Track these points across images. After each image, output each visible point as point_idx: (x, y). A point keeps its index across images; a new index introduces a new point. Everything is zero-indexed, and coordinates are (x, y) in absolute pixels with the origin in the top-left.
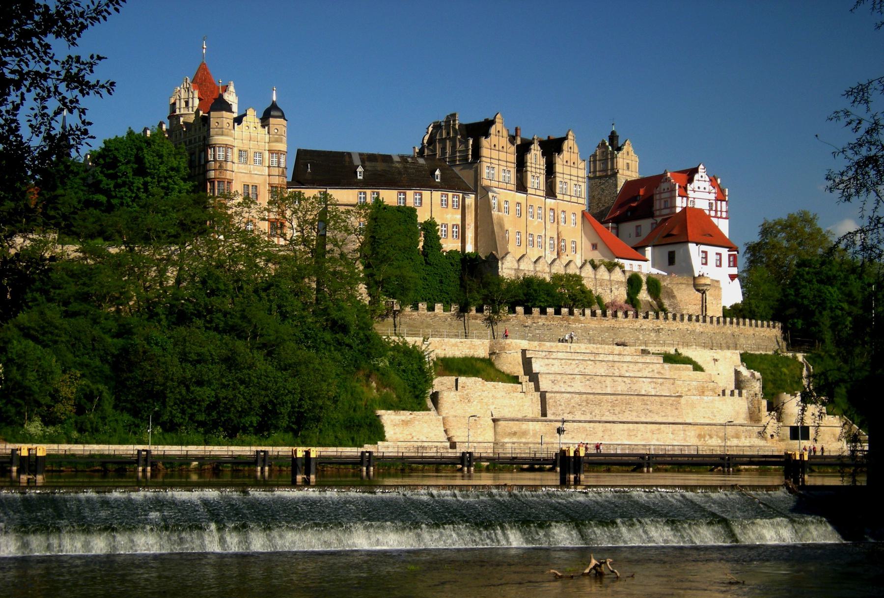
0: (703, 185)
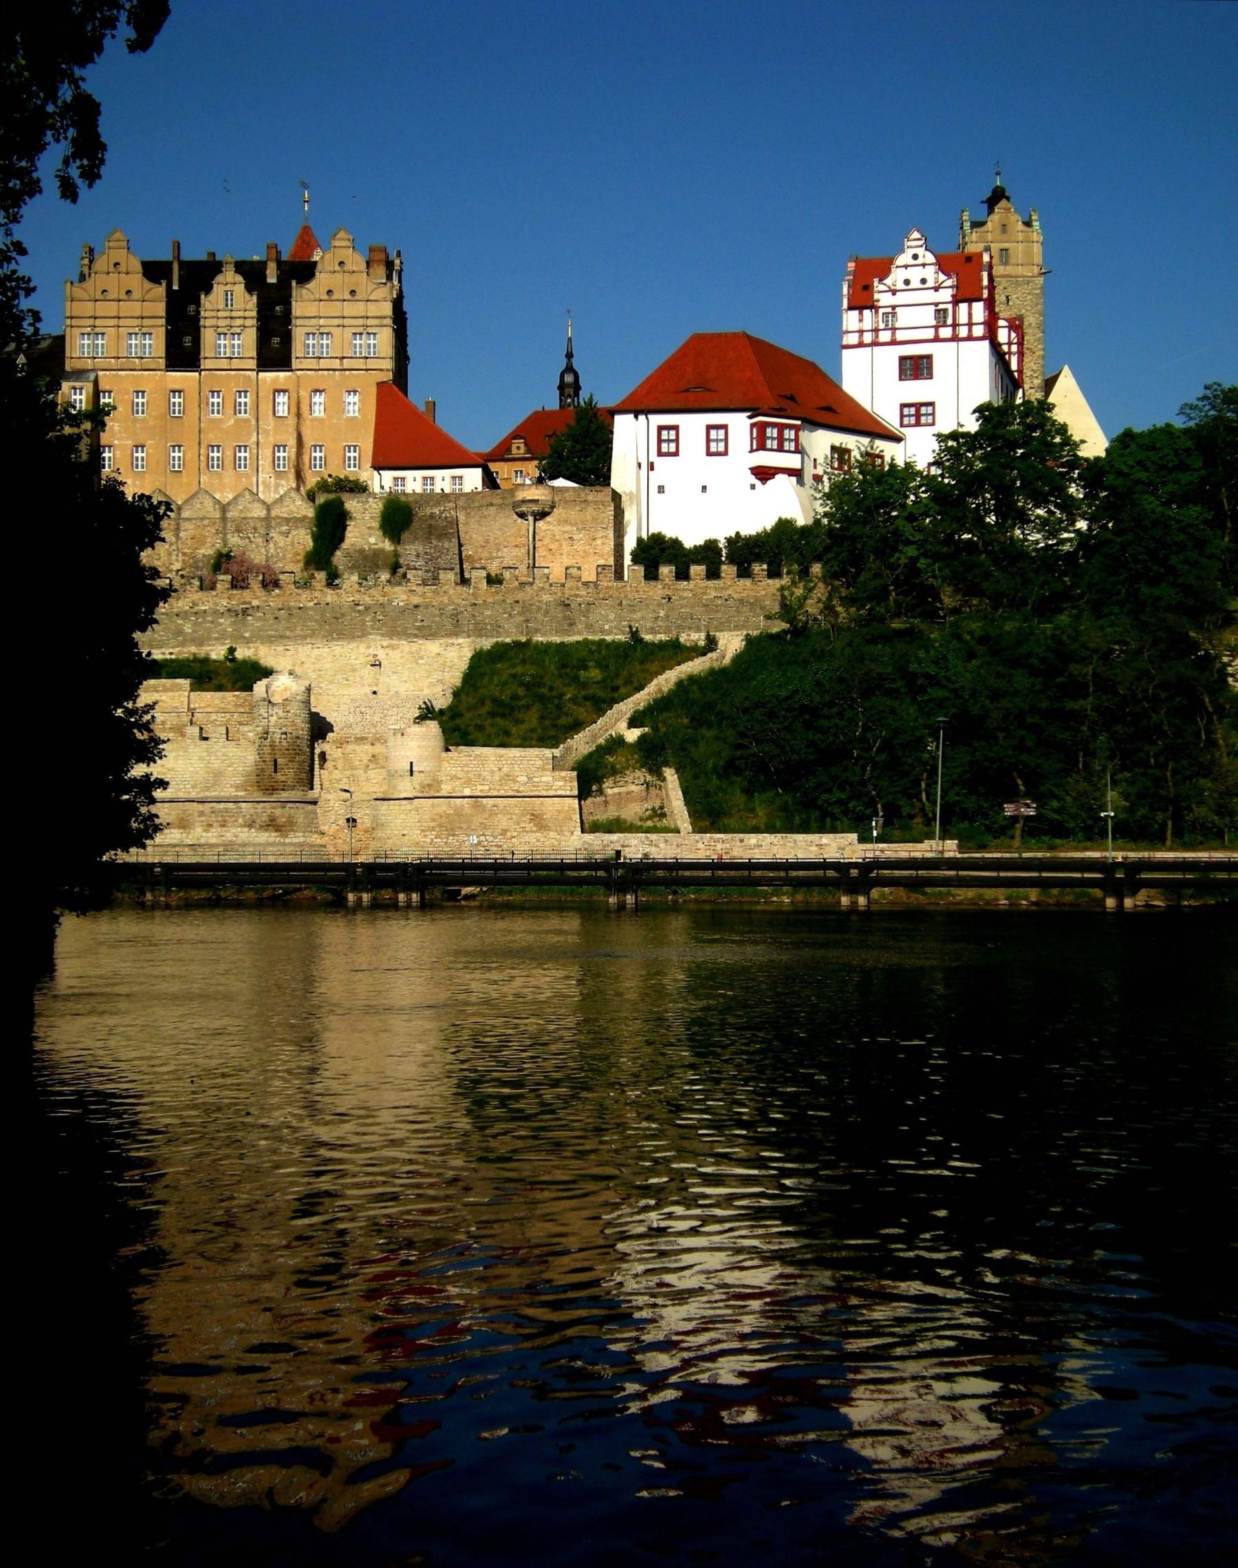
0: (915, 275)
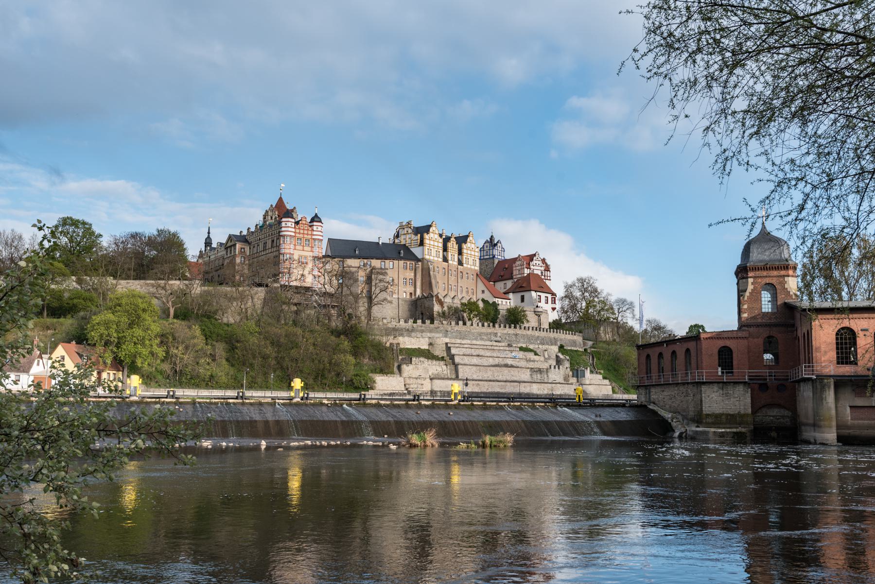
0: (538, 262)
